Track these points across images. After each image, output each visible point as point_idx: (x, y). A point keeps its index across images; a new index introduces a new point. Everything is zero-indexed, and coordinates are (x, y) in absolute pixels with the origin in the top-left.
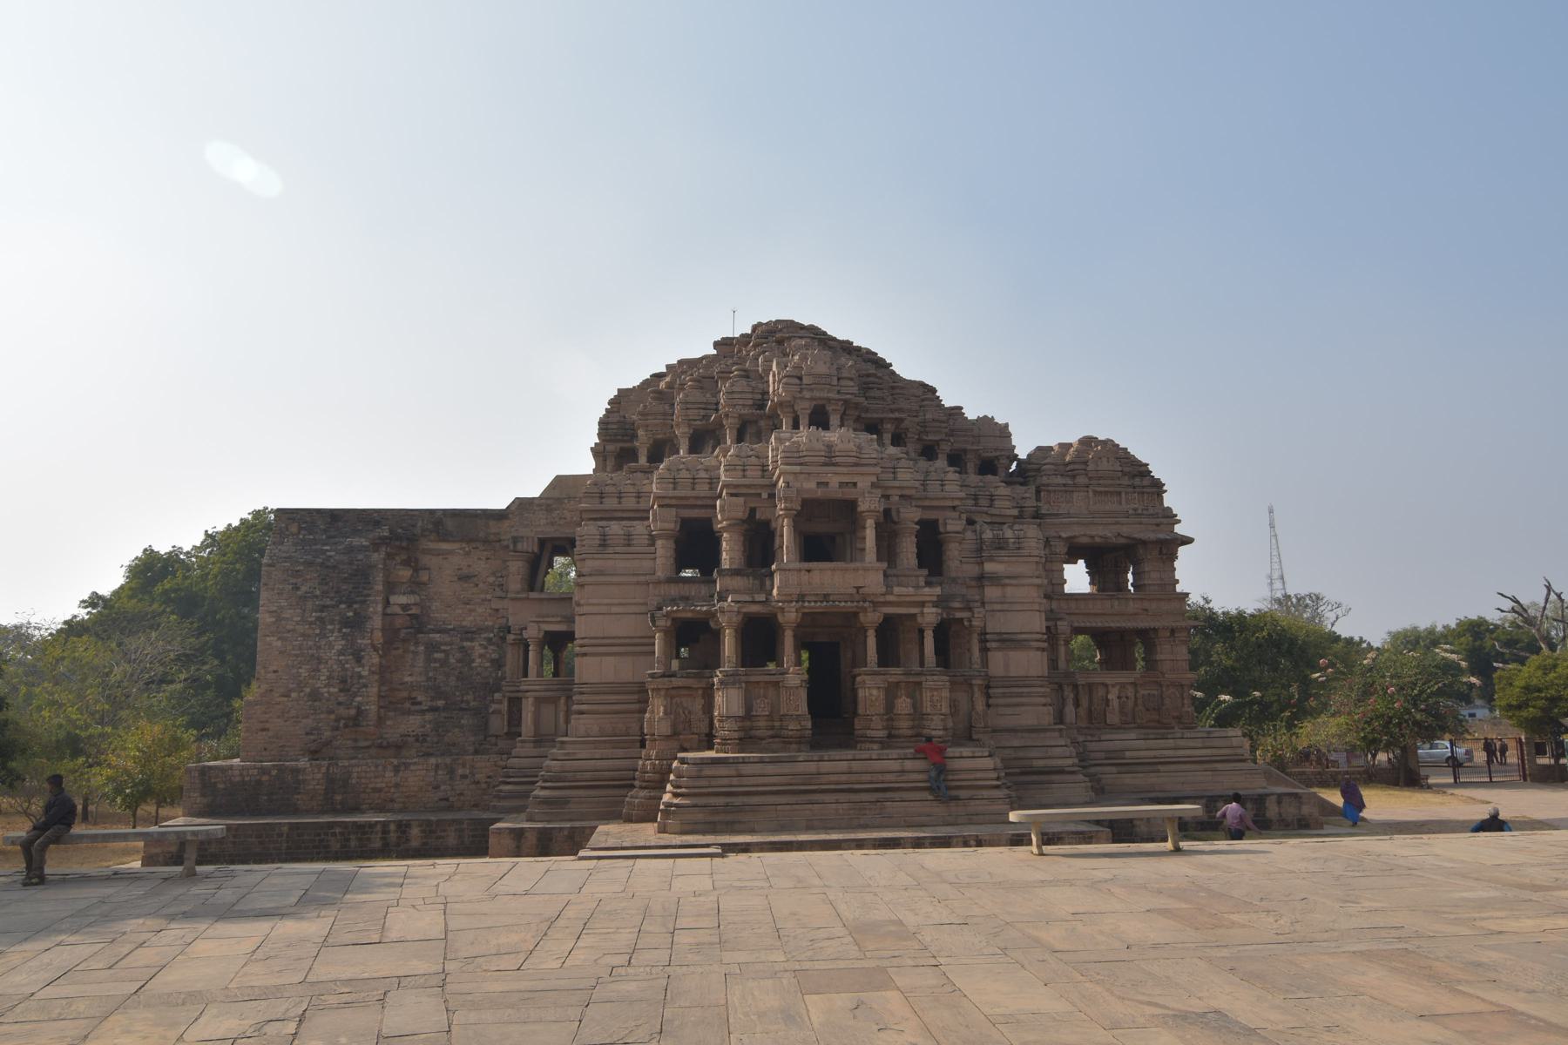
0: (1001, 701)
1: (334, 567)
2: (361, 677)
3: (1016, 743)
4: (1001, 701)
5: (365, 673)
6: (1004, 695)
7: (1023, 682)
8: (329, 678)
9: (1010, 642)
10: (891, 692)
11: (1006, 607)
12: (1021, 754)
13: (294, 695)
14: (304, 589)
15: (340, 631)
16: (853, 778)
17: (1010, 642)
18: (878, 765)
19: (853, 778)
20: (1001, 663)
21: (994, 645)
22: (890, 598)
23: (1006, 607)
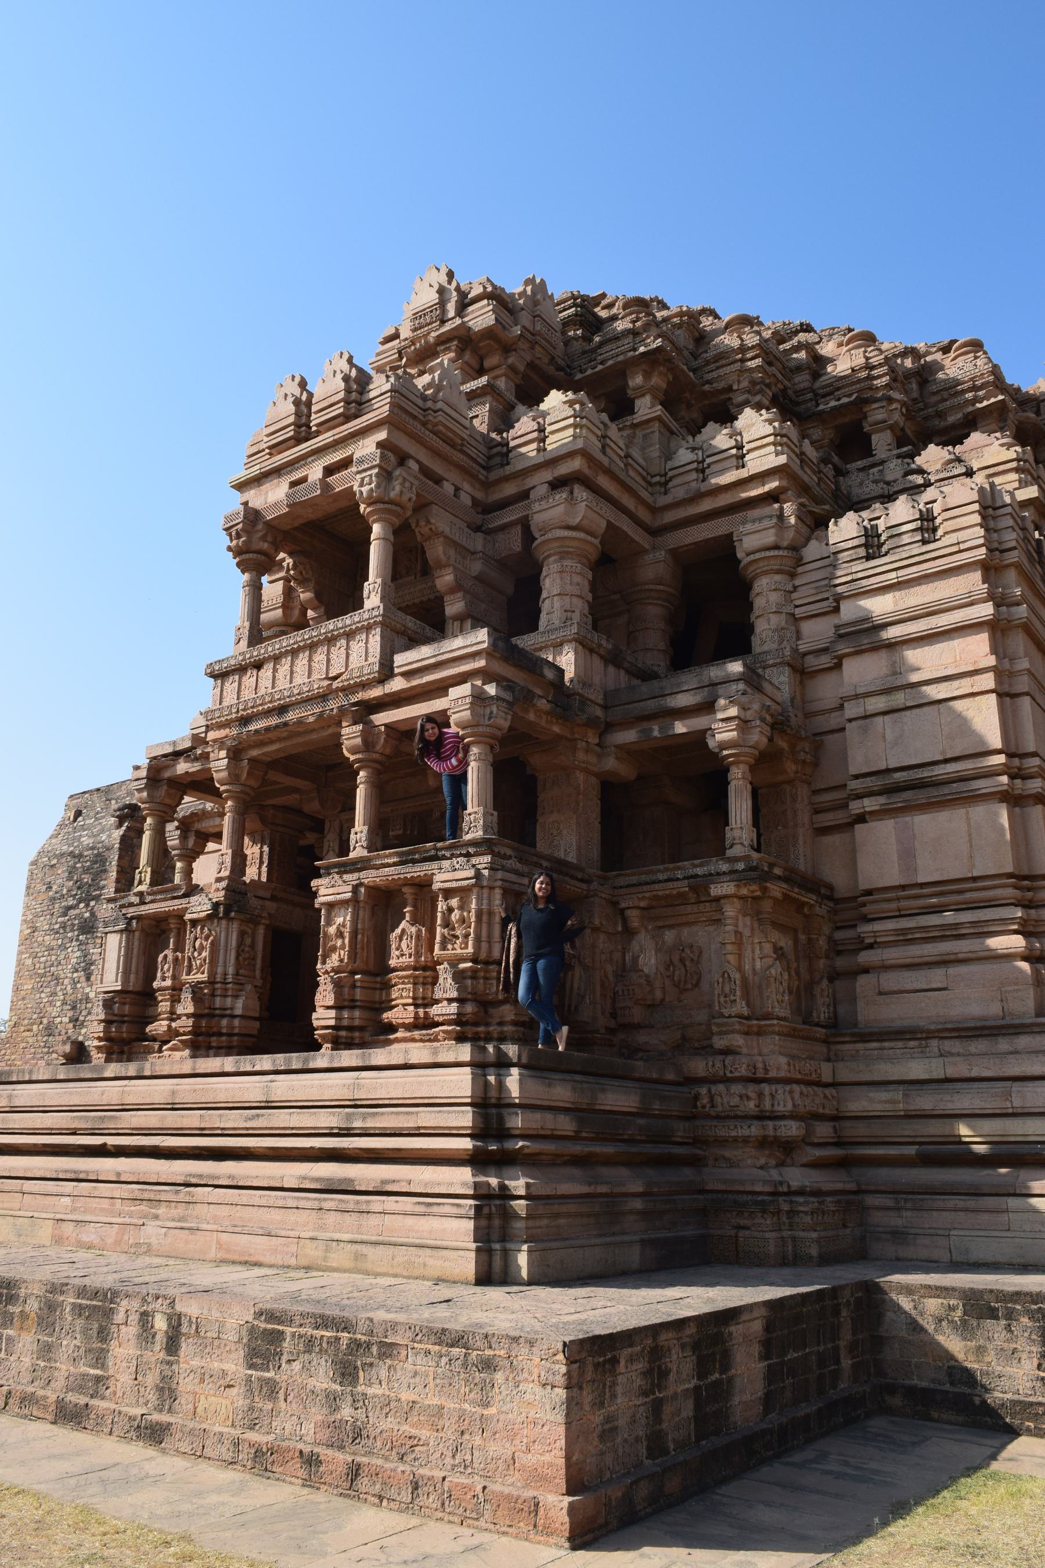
0: (892, 955)
1: (81, 855)
2: (87, 1000)
3: (917, 1069)
4: (892, 955)
5: (92, 995)
6: (905, 938)
7: (962, 891)
8: (64, 1003)
9: (916, 789)
10: (381, 907)
11: (899, 699)
12: (925, 1102)
13: (35, 1028)
14: (55, 888)
15: (77, 940)
16: (172, 1119)
17: (916, 789)
18: (187, 1090)
19: (172, 1119)
20: (885, 852)
21: (870, 804)
22: (397, 684)
23: (899, 699)
